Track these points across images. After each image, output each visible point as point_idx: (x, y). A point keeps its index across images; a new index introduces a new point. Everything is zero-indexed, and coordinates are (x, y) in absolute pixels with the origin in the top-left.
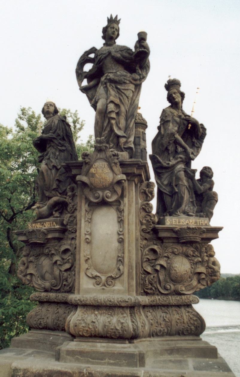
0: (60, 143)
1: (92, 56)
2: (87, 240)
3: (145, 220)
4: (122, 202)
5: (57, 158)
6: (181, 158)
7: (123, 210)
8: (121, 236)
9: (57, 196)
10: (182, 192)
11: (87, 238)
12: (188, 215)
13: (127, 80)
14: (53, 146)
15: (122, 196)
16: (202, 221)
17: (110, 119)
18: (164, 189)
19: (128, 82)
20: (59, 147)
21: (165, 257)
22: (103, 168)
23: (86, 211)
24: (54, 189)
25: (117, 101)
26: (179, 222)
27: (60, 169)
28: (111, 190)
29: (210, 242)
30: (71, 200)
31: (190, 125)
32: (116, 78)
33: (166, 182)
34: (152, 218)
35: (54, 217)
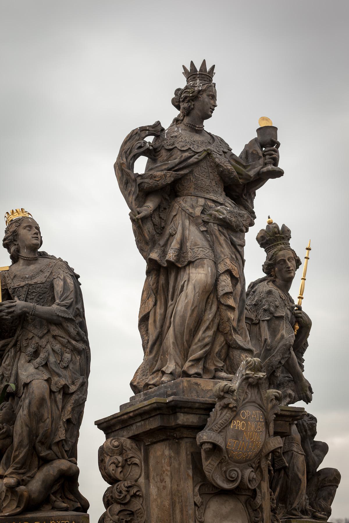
7: (261, 507)
10: (298, 468)
14: (54, 337)
20: (74, 342)
22: (257, 422)
23: (195, 504)
24: (58, 443)
27: (73, 393)
30: (121, 472)
32: (233, 219)
35: (54, 508)
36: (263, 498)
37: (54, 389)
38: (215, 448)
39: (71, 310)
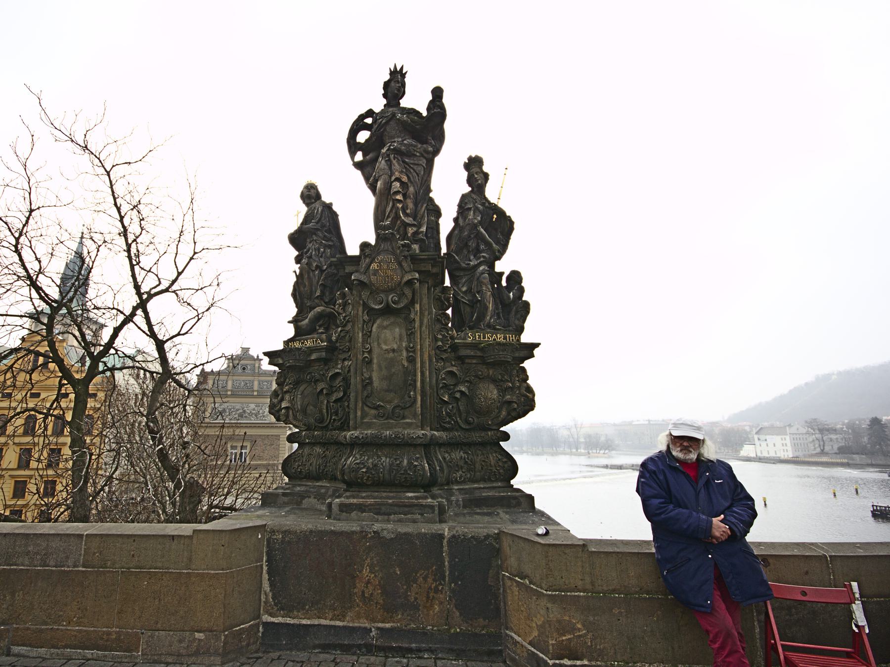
0: (325, 236)
1: (369, 121)
2: (367, 359)
3: (441, 334)
4: (412, 309)
5: (321, 257)
6: (484, 257)
7: (414, 320)
8: (411, 354)
9: (322, 306)
11: (366, 357)
12: (495, 329)
13: (417, 152)
15: (412, 302)
16: (512, 337)
17: (395, 202)
18: (462, 297)
19: (418, 154)
21: (467, 381)
25: (405, 179)
26: (484, 338)
27: (325, 270)
28: (398, 293)
29: (523, 363)
31: (495, 216)
33: (464, 289)
34: (450, 333)
36: (416, 314)
37: (314, 269)
38: (362, 284)
39: (319, 224)
